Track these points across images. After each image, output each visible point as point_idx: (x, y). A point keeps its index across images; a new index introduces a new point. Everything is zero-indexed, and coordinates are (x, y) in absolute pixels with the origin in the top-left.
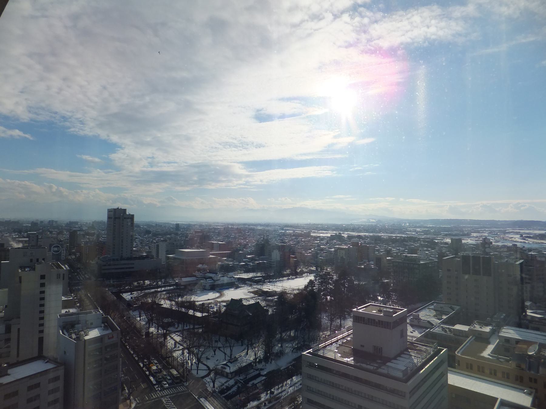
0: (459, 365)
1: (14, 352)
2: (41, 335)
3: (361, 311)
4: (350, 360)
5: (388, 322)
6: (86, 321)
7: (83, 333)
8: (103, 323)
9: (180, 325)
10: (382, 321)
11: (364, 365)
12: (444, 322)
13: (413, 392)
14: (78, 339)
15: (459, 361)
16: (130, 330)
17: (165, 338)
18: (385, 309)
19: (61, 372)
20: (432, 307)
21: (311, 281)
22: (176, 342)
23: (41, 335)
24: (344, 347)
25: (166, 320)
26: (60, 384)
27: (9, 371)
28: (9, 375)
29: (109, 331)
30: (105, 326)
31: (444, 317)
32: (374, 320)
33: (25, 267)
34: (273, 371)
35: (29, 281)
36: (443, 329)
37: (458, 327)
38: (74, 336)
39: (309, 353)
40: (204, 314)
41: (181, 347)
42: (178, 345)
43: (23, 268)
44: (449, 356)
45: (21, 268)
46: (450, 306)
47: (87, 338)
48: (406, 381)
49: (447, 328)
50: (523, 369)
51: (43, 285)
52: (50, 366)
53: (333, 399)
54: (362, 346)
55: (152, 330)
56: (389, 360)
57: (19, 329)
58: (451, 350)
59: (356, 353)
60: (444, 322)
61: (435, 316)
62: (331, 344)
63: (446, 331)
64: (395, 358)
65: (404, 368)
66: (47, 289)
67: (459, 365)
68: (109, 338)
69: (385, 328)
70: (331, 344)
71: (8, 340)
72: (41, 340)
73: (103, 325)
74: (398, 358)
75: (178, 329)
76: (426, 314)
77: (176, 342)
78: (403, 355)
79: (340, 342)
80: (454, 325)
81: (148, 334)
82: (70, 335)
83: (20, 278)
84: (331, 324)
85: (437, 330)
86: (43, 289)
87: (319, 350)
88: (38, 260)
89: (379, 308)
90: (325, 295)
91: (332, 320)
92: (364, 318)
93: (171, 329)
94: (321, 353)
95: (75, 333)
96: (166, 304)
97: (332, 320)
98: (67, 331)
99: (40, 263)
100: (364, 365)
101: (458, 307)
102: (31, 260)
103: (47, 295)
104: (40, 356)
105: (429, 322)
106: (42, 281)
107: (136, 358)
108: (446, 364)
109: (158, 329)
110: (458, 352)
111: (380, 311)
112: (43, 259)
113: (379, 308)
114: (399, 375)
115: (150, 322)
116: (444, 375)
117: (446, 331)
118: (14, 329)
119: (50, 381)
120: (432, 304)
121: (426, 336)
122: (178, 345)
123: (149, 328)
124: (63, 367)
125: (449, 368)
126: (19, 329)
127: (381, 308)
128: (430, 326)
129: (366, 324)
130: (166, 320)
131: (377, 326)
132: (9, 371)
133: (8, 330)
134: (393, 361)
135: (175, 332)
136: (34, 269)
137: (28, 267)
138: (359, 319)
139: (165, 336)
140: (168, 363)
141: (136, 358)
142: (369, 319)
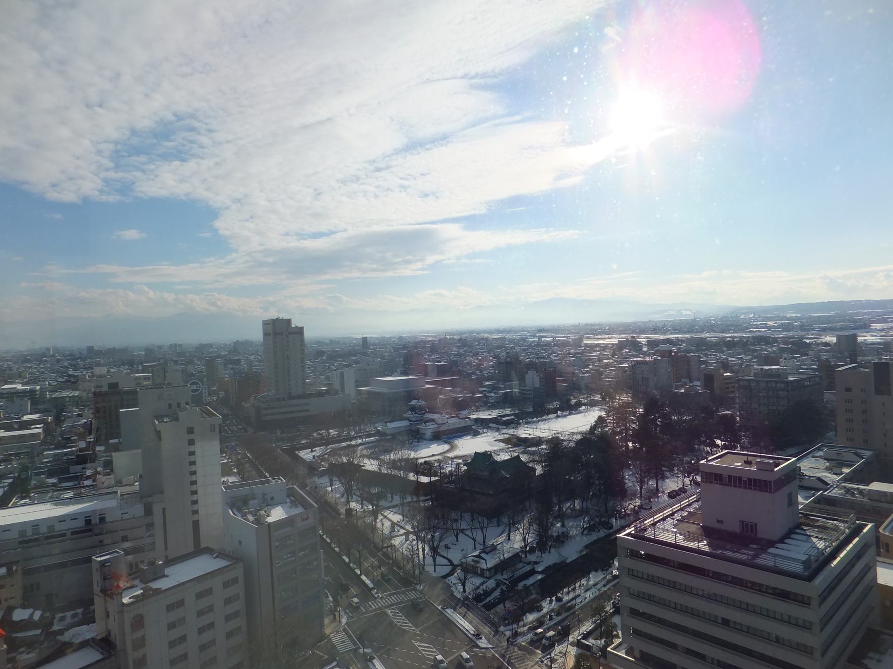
0: (888, 551)
1: (160, 545)
2: (196, 517)
3: (713, 463)
4: (703, 545)
5: (765, 482)
6: (264, 495)
7: (263, 512)
8: (288, 496)
9: (395, 497)
10: (755, 480)
11: (728, 553)
12: (848, 479)
13: (823, 597)
14: (258, 521)
15: (887, 545)
16: (327, 508)
17: (376, 518)
18: (758, 460)
19: (238, 572)
20: (821, 453)
21: (600, 418)
22: (393, 524)
23: (196, 517)
24: (686, 525)
25: (375, 490)
26: (239, 589)
27: (167, 571)
28: (167, 576)
29: (299, 510)
30: (292, 502)
31: (846, 470)
32: (740, 478)
33: (163, 416)
34: (555, 564)
35: (171, 436)
36: (848, 491)
37: (876, 486)
38: (251, 518)
39: (629, 534)
40: (433, 479)
41: (402, 531)
42: (397, 528)
43: (159, 417)
45: (157, 418)
46: (852, 450)
47: (270, 520)
48: (810, 578)
49: (854, 489)
51: (191, 442)
52: (220, 563)
53: (676, 608)
54: (718, 521)
55: (353, 505)
56: (772, 544)
57: (164, 510)
59: (708, 532)
60: (845, 480)
61: (827, 469)
62: (664, 519)
63: (853, 495)
64: (781, 541)
65: (804, 558)
66: (197, 448)
67: (888, 551)
68: (303, 520)
70: (664, 519)
71: (150, 526)
72: (196, 525)
73: (288, 500)
74: (787, 541)
75: (394, 503)
76: (812, 466)
77: (393, 524)
78: (793, 536)
79: (677, 516)
80: (868, 484)
81: (349, 512)
82: (244, 515)
83: (158, 434)
84: (641, 488)
85: (835, 493)
86: (192, 448)
87: (645, 530)
88: (179, 405)
89: (745, 458)
90: (626, 441)
91: (642, 483)
93: (382, 503)
94: (649, 534)
95: (251, 513)
96: (370, 465)
97: (642, 483)
98: (239, 510)
99: (185, 409)
100: (728, 553)
101: (868, 453)
102: (170, 406)
103: (198, 458)
104: (199, 551)
105: (819, 479)
106: (191, 437)
107: (337, 549)
108: (872, 550)
109: (362, 504)
110: (884, 529)
112: (187, 403)
113: (745, 458)
114: (798, 568)
115: (348, 493)
116: (870, 569)
117: (853, 495)
118: (157, 509)
119: (226, 585)
120: (819, 449)
121: (818, 501)
122: (397, 528)
123: (348, 502)
124: (240, 564)
125: (878, 559)
126: (164, 510)
127: (750, 458)
128: (821, 485)
130: (375, 490)
131: (746, 488)
132: (167, 571)
133: (148, 511)
134: (778, 545)
135: (388, 508)
136: (177, 419)
137: (167, 416)
138: (714, 477)
139: (375, 514)
140: (386, 555)
141: (337, 549)
142: (730, 477)
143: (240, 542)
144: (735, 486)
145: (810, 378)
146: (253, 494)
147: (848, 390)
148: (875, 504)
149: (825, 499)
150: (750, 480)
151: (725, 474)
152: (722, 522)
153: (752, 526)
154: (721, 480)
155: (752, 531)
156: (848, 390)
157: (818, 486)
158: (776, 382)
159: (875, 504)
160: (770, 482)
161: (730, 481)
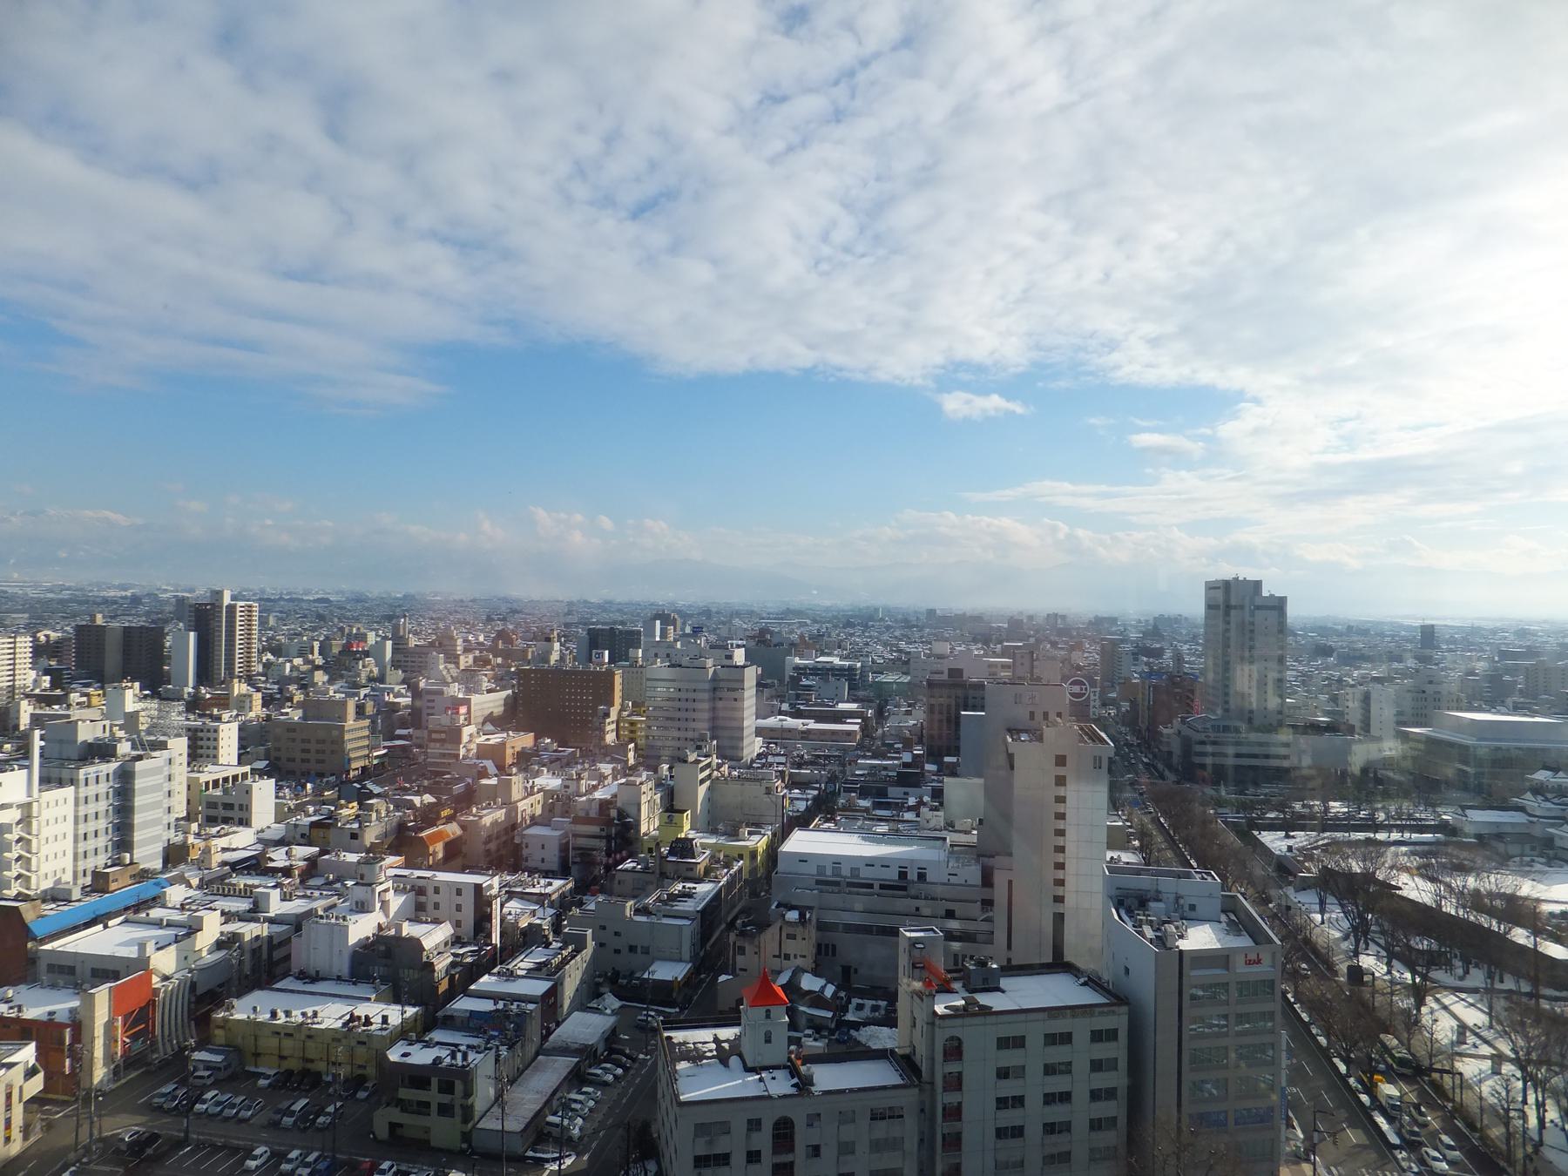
1: (1000, 937)
2: (1060, 908)
6: (1178, 898)
7: (1171, 928)
8: (1223, 911)
9: (1473, 971)
14: (1161, 941)
17: (1420, 1002)
19: (1118, 1020)
22: (1463, 1028)
25: (1423, 944)
27: (1004, 983)
29: (1244, 942)
30: (1230, 923)
33: (1019, 731)
35: (1032, 762)
38: (1149, 932)
41: (1485, 1050)
42: (1471, 1039)
45: (1010, 731)
47: (1184, 945)
51: (1060, 781)
52: (1089, 997)
55: (1367, 961)
57: (1010, 882)
66: (1071, 791)
68: (1249, 963)
72: (1059, 918)
73: (1223, 918)
75: (1467, 983)
77: (1463, 1028)
81: (1356, 973)
82: (1138, 925)
83: (1011, 757)
86: (1061, 791)
88: (1046, 715)
93: (1438, 975)
95: (1150, 923)
96: (1416, 889)
98: (1130, 912)
99: (1055, 724)
102: (1032, 714)
103: (1070, 808)
104: (1058, 964)
106: (1061, 771)
107: (1323, 1040)
109: (1389, 964)
112: (1059, 715)
115: (1360, 933)
118: (1000, 879)
119: (1097, 1036)
122: (1471, 1039)
123: (1356, 954)
124: (1124, 1009)
126: (1010, 882)
130: (1423, 944)
132: (1004, 983)
135: (1455, 990)
136: (1040, 739)
137: (1026, 731)
139: (1419, 994)
140: (1438, 1088)
141: (1323, 1040)
143: (1127, 971)
146: (1158, 892)
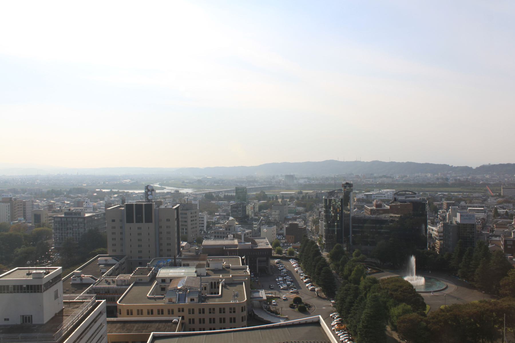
10: (31, 286)
18: (34, 272)
32: (21, 286)
44: (108, 308)
50: (174, 303)
54: (5, 320)
58: (111, 300)
67: (120, 314)
69: (35, 292)
89: (27, 271)
92: (8, 286)
108: (105, 315)
110: (119, 302)
111: (28, 274)
113: (27, 271)
127: (31, 271)
129: (11, 292)
131: (25, 292)
142: (14, 286)
144: (18, 292)
145: (98, 215)
147: (113, 221)
148: (119, 287)
149: (94, 289)
150: (28, 286)
151: (11, 284)
152: (8, 320)
153: (29, 317)
154: (8, 289)
155: (29, 322)
156: (113, 221)
157: (90, 282)
158: (78, 218)
159: (119, 287)
160: (41, 286)
161: (14, 289)
